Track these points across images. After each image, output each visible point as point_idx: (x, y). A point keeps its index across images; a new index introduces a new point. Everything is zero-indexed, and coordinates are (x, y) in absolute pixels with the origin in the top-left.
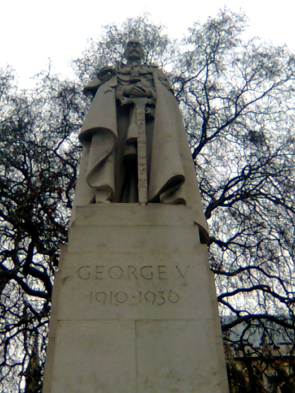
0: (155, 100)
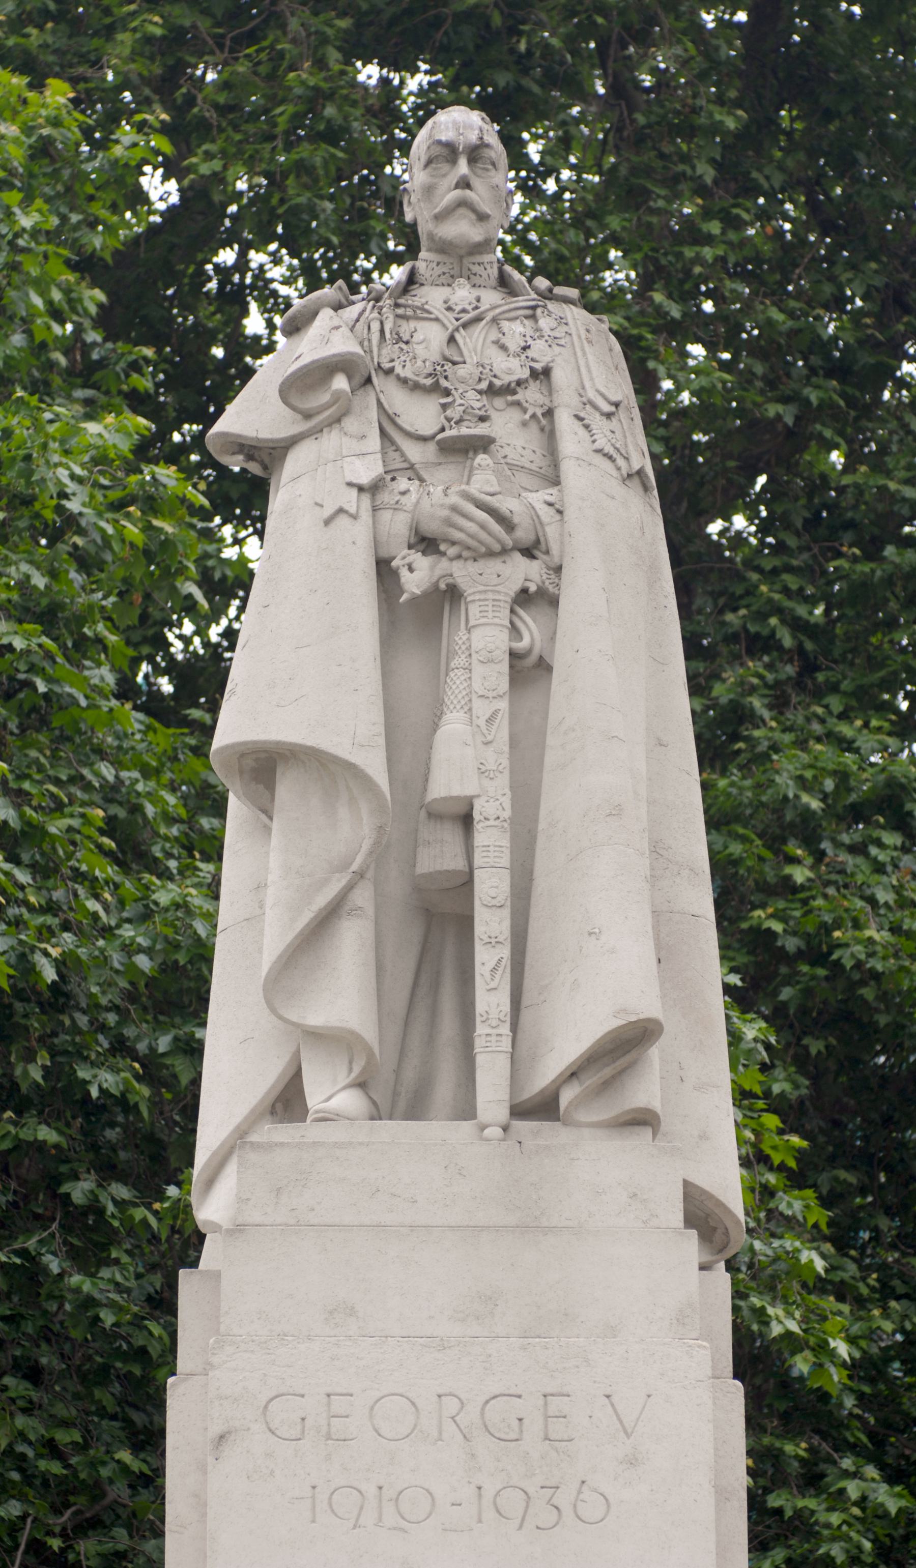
0: (558, 569)
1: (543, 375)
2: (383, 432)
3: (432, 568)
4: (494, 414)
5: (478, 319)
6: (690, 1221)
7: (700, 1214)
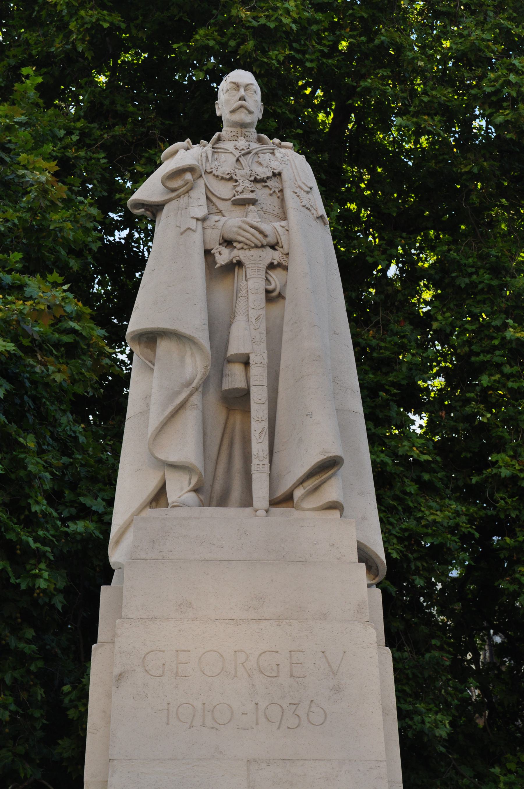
0: (287, 254)
1: (277, 175)
2: (207, 198)
3: (230, 253)
4: (257, 190)
5: (249, 153)
6: (360, 560)
7: (364, 556)
